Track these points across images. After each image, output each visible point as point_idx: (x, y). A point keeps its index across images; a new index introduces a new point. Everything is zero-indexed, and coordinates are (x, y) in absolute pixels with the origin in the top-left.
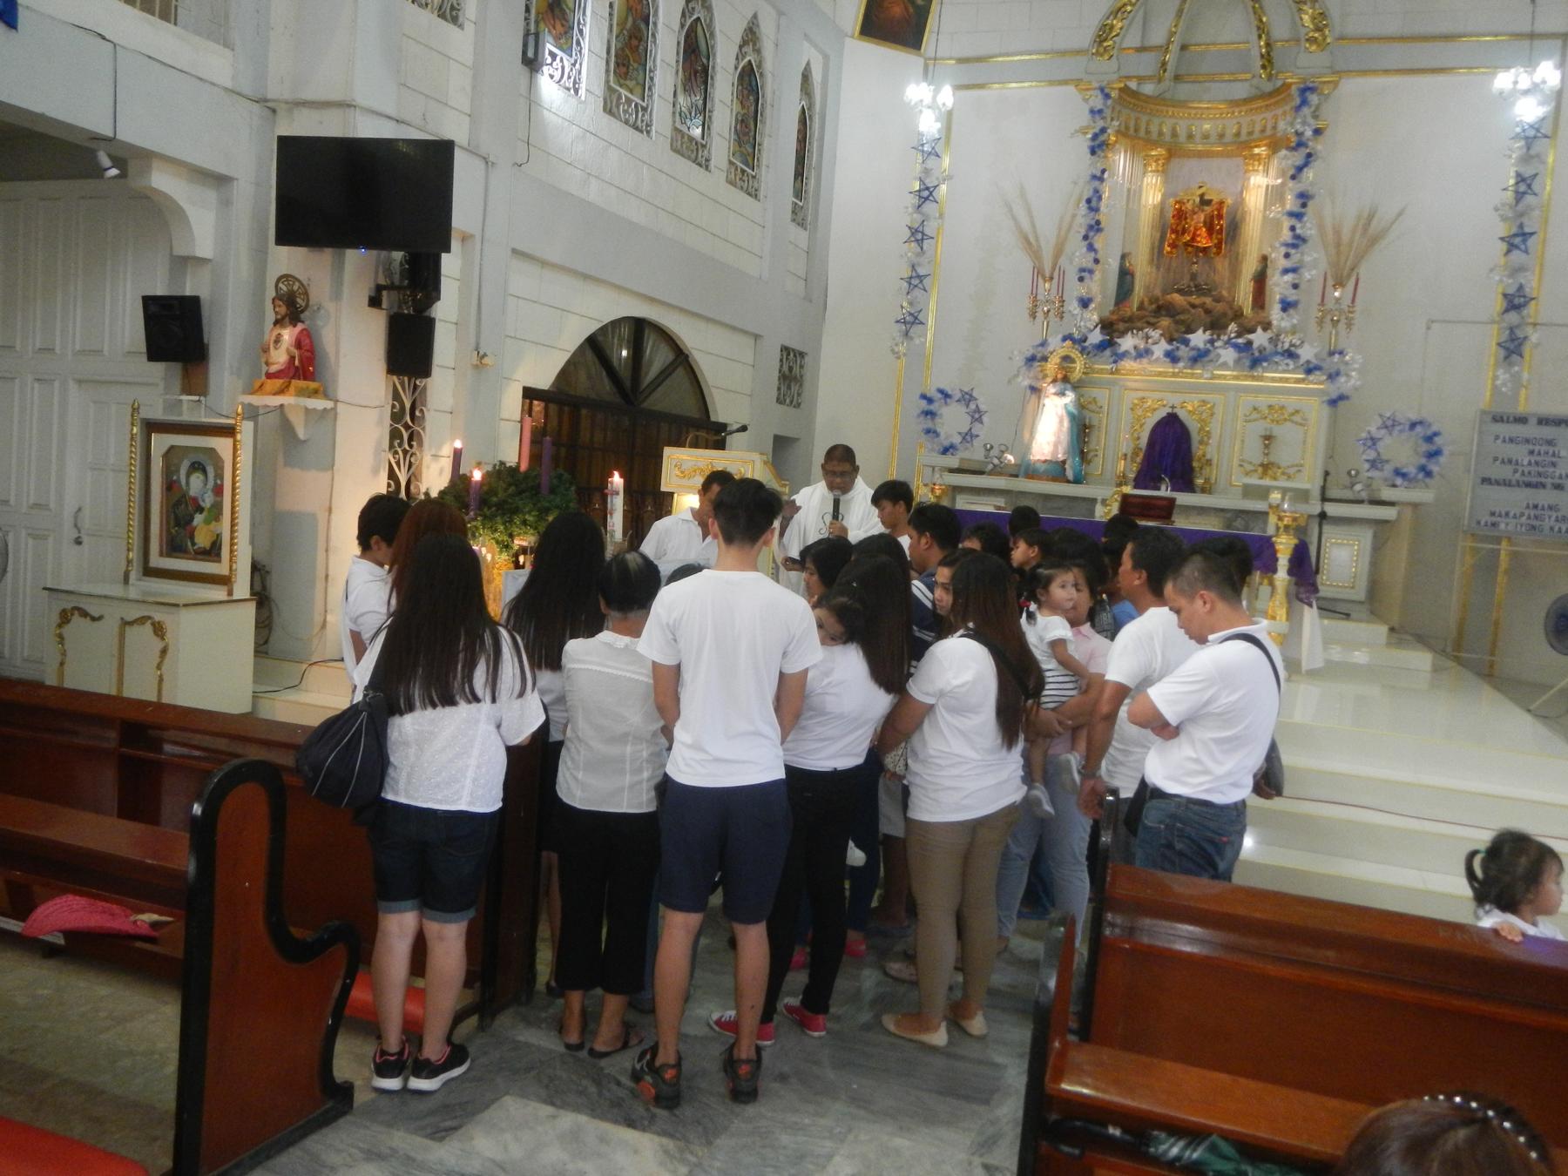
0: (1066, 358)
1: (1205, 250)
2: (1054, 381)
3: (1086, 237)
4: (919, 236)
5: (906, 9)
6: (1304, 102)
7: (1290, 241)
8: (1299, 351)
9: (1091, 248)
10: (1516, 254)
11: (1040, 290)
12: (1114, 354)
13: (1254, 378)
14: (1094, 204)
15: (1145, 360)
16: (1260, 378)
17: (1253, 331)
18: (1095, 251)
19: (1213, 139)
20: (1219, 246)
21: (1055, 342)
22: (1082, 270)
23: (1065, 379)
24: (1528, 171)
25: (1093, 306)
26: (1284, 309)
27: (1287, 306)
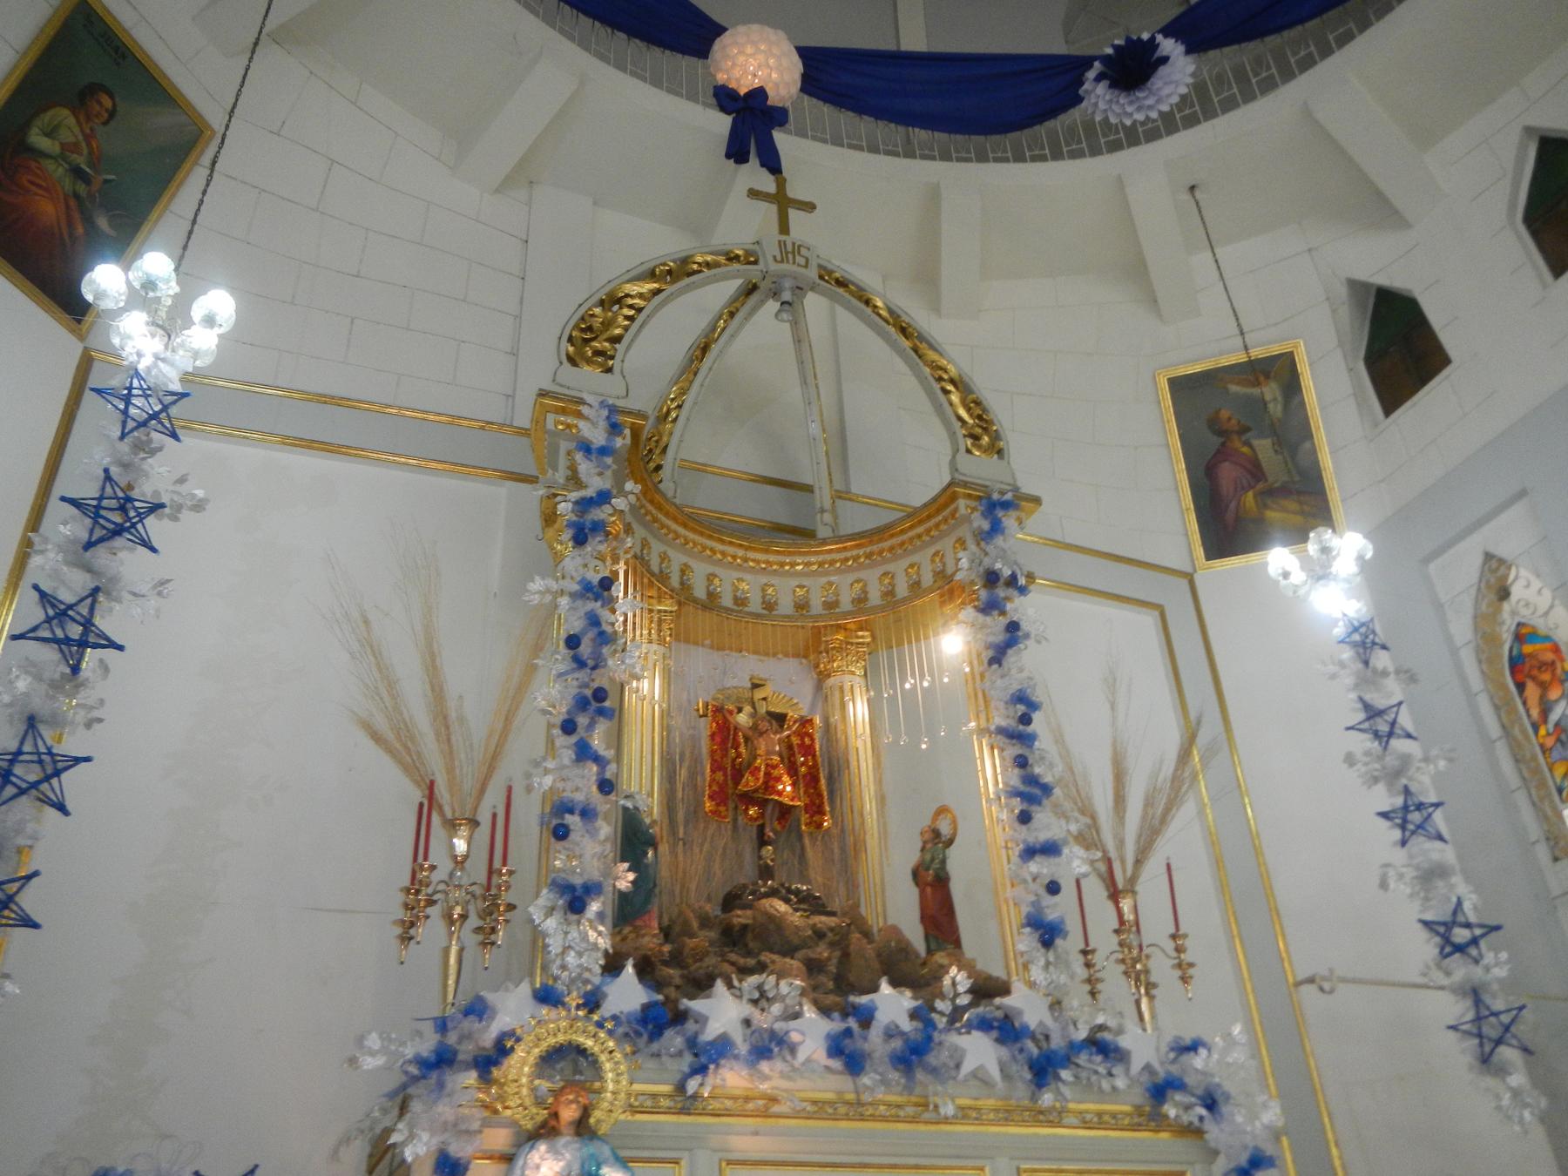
0: (566, 1060)
1: (785, 812)
2: (546, 1131)
3: (568, 727)
4: (75, 631)
5: (70, 224)
6: (996, 528)
7: (1022, 788)
8: (1124, 1042)
9: (584, 752)
10: (1420, 843)
11: (437, 855)
12: (692, 1043)
13: (1041, 1116)
14: (585, 649)
15: (779, 1065)
16: (1053, 1117)
17: (1005, 990)
18: (597, 759)
19: (755, 605)
20: (815, 809)
21: (512, 1008)
22: (565, 808)
23: (582, 1128)
24: (1380, 702)
25: (594, 907)
26: (1047, 943)
27: (1048, 934)
